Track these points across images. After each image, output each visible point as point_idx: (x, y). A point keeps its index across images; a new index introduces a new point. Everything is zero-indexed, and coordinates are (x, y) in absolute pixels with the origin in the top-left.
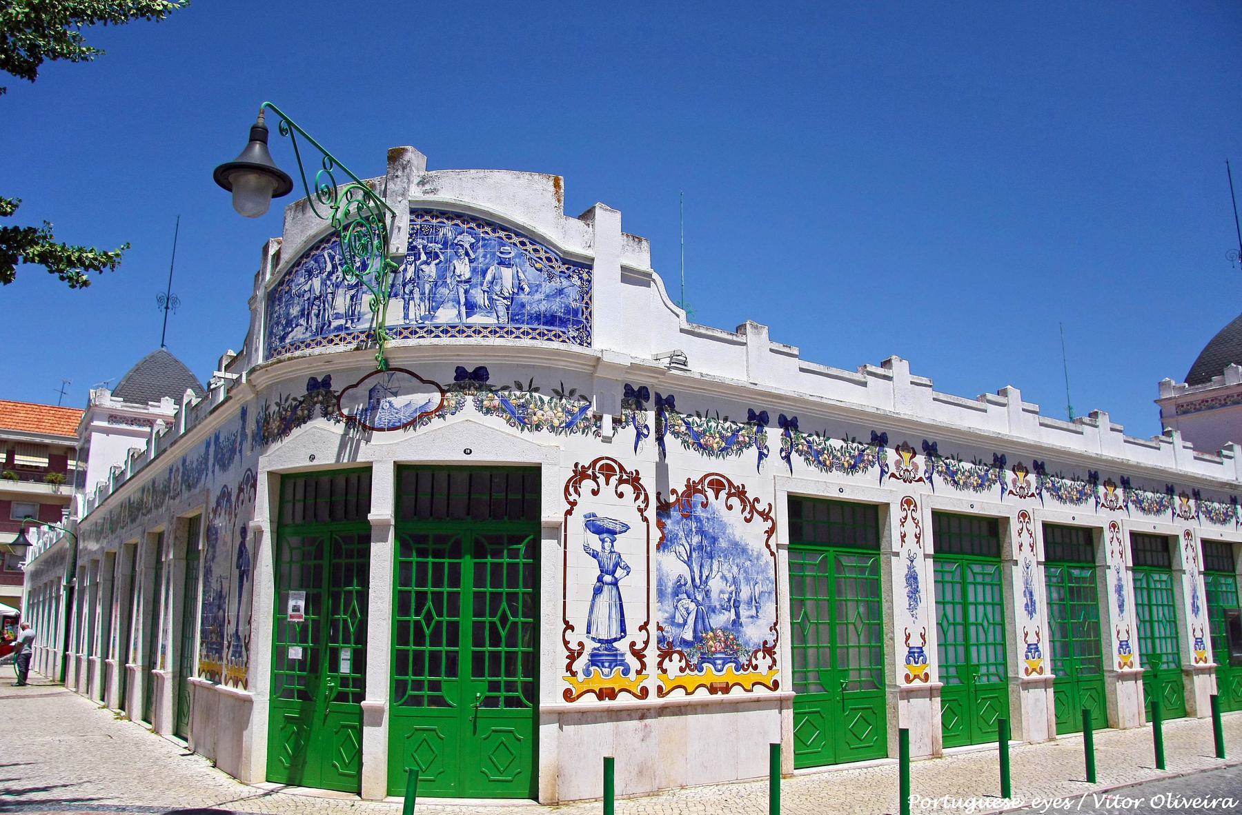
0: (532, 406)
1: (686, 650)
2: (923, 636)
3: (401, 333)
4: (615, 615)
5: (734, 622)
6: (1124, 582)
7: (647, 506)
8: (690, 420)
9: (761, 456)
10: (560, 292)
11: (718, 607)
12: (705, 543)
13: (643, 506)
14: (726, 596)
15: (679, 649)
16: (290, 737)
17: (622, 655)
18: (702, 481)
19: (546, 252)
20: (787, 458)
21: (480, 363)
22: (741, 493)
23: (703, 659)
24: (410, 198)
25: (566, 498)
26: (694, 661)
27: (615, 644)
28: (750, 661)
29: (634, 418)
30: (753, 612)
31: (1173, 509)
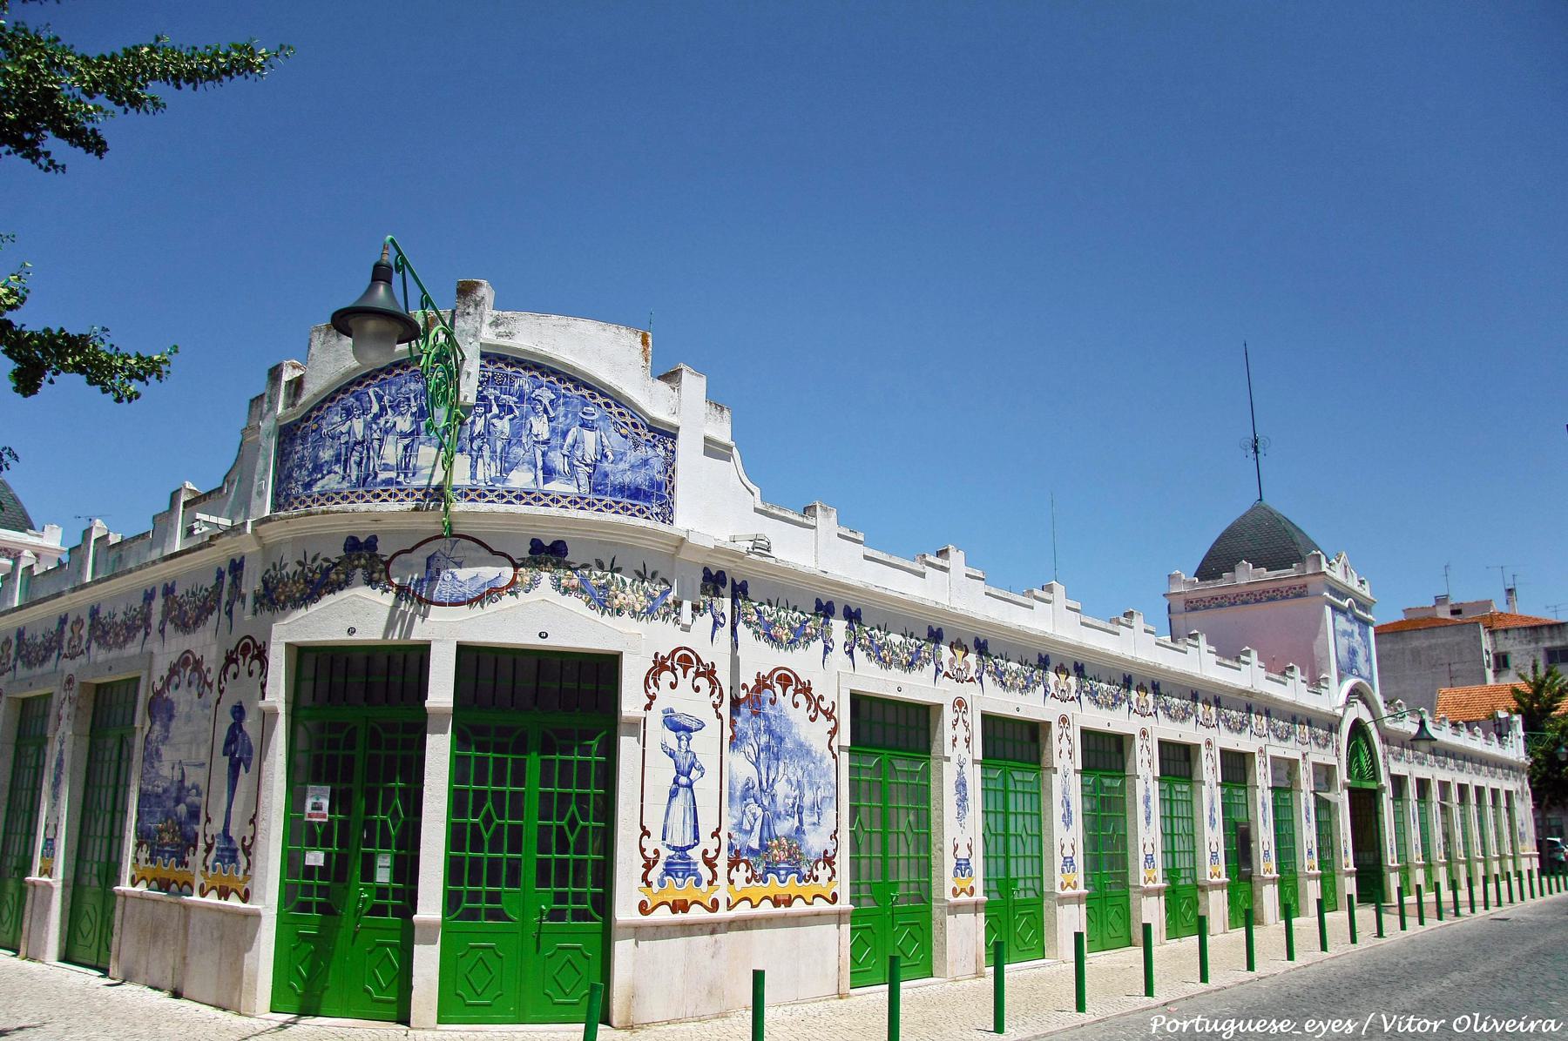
0: (613, 588)
1: (752, 859)
2: (969, 847)
3: (467, 495)
4: (689, 822)
5: (797, 829)
6: (1151, 793)
7: (721, 702)
8: (762, 608)
9: (827, 650)
10: (645, 462)
11: (783, 813)
12: (772, 743)
13: (717, 702)
14: (791, 801)
15: (745, 858)
16: (306, 957)
17: (695, 864)
18: (771, 675)
19: (632, 417)
20: (850, 653)
21: (559, 537)
22: (806, 690)
23: (768, 870)
24: (482, 341)
25: (646, 691)
26: (760, 871)
27: (689, 852)
28: (811, 871)
29: (711, 605)
30: (815, 819)
31: (1197, 716)
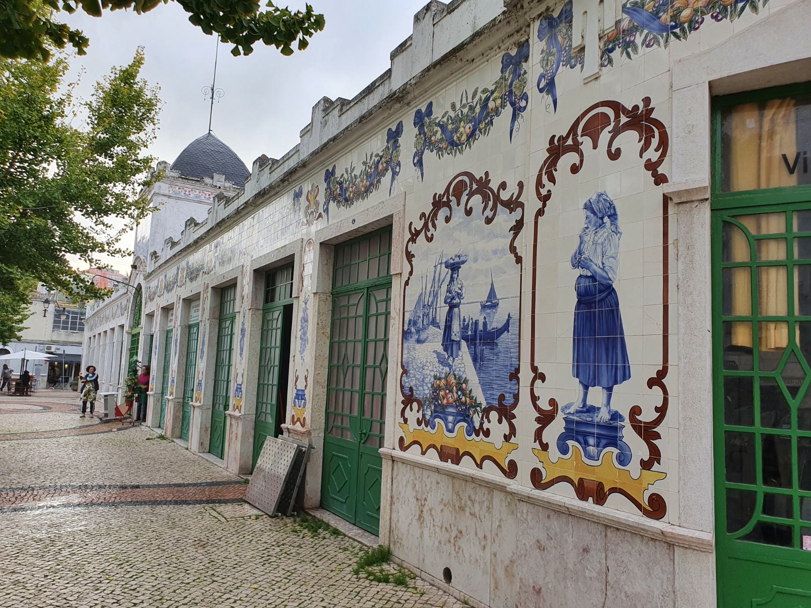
7: (664, 155)
